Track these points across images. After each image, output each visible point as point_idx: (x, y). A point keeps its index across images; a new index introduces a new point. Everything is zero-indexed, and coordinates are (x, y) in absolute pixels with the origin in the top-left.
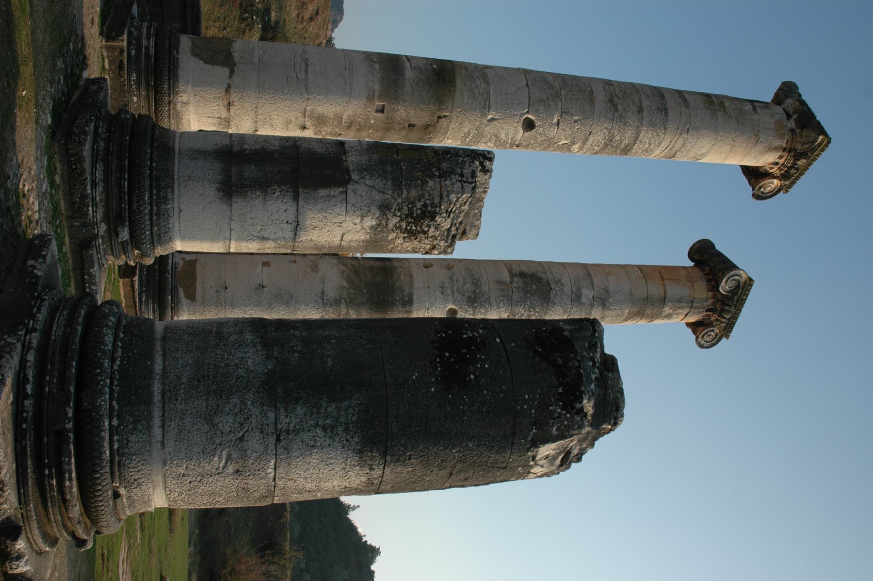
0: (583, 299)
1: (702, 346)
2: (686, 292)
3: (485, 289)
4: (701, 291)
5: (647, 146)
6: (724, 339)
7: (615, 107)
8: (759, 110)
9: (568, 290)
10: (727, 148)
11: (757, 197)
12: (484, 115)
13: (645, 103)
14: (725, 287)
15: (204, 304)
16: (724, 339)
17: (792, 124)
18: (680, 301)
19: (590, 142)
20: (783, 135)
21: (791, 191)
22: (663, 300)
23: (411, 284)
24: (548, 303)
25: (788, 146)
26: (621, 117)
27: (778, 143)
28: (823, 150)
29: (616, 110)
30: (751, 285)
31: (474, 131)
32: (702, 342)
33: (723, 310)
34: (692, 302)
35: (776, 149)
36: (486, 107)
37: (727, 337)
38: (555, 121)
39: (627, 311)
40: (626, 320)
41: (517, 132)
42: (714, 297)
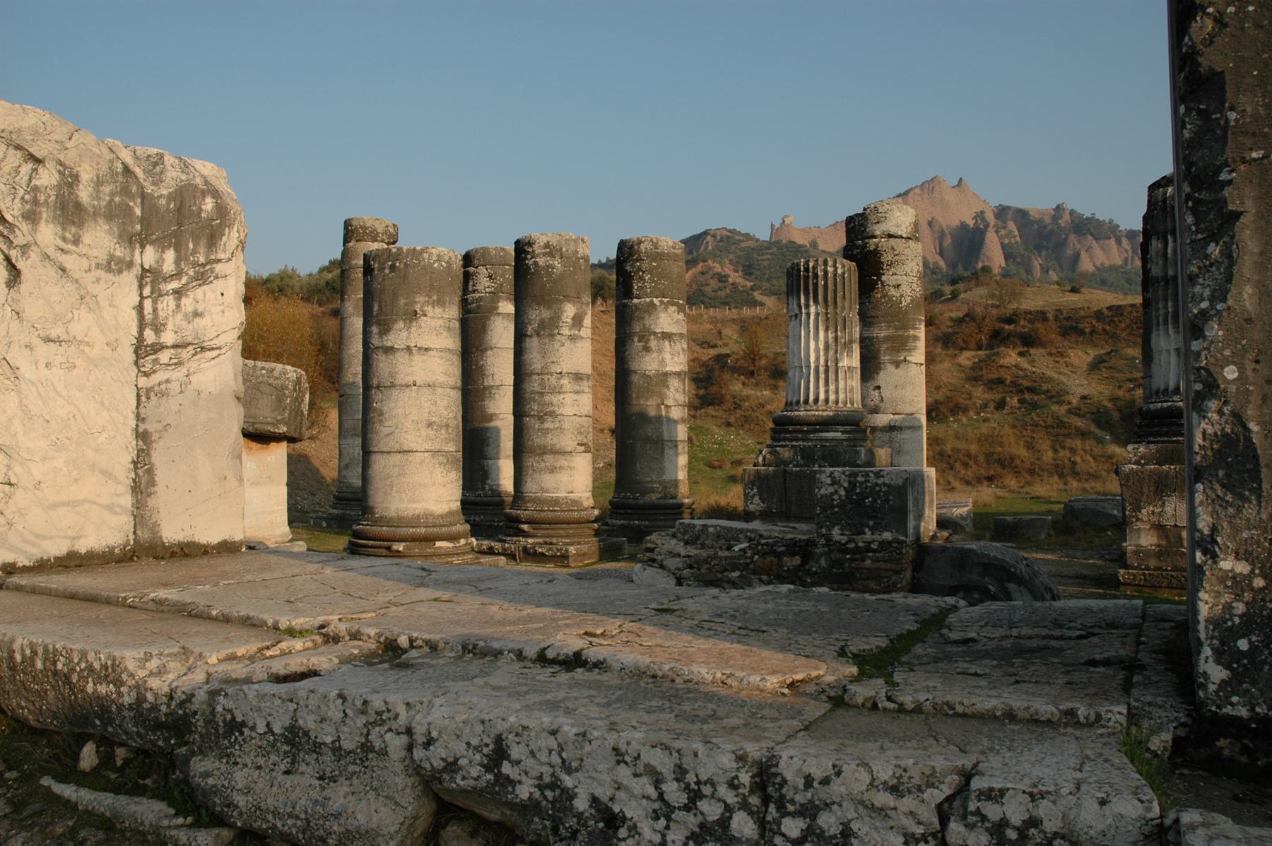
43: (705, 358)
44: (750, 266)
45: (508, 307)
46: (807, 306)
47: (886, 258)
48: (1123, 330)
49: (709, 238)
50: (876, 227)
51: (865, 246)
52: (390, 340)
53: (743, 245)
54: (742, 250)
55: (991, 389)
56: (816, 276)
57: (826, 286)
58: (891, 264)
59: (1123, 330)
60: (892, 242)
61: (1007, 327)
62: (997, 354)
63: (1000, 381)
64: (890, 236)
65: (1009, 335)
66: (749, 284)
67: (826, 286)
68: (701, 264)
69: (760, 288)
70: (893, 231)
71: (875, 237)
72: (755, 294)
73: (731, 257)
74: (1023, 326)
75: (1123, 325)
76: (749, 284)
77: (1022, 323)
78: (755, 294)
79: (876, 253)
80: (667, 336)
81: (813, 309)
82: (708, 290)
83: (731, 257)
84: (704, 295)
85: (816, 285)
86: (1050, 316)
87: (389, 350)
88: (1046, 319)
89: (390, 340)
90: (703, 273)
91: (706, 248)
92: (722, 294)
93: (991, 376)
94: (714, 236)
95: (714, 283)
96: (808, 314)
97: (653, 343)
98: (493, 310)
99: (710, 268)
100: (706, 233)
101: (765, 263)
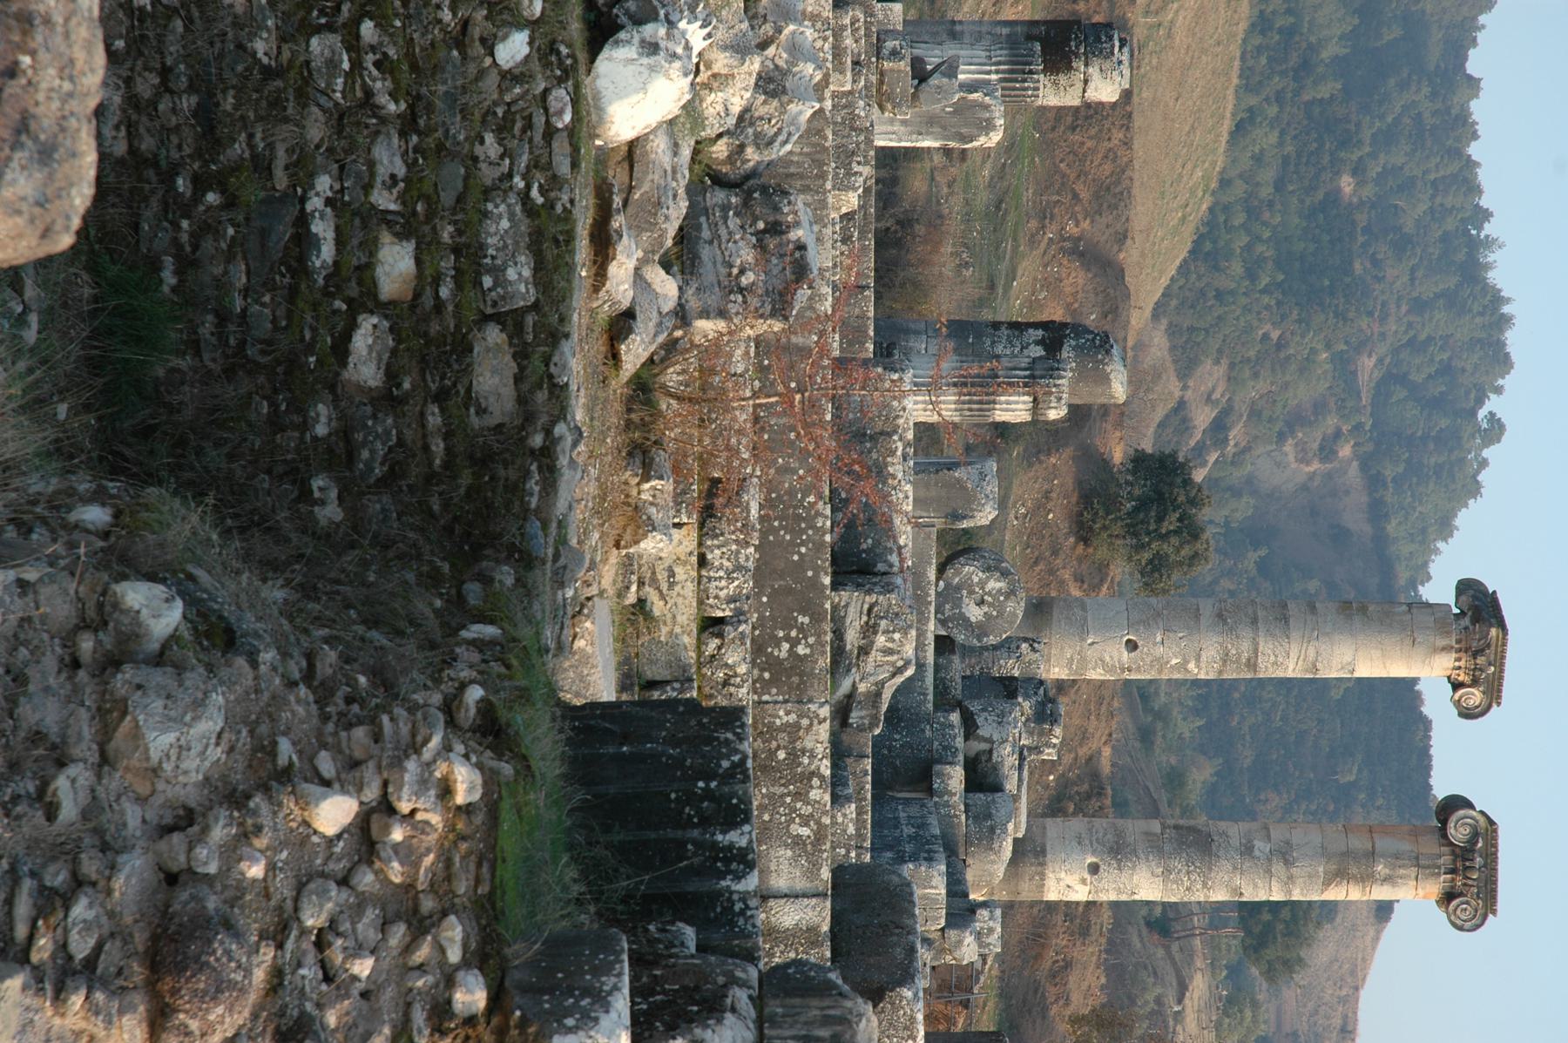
0: (1257, 853)
1: (1461, 928)
2: (1406, 846)
3: (1131, 839)
4: (1430, 846)
5: (1272, 658)
6: (1491, 916)
7: (1225, 622)
8: (1414, 611)
9: (1235, 842)
10: (1376, 653)
11: (1467, 714)
12: (1084, 640)
13: (1260, 613)
14: (1458, 832)
16: (1491, 916)
17: (1466, 621)
18: (1397, 856)
19: (1204, 658)
20: (1448, 633)
21: (1504, 700)
22: (1372, 855)
23: (1044, 834)
24: (1210, 855)
25: (1463, 645)
26: (1231, 629)
27: (1441, 642)
28: (1504, 644)
29: (1225, 622)
30: (1495, 831)
31: (1077, 657)
32: (1459, 922)
33: (1466, 868)
34: (1417, 858)
36: (1083, 630)
37: (1494, 912)
38: (1159, 639)
39: (1321, 869)
41: (1121, 654)
42: (1453, 853)
46: (997, 72)
47: (1062, 79)
50: (1097, 68)
51: (1077, 55)
56: (1024, 81)
57: (1015, 89)
58: (1055, 83)
60: (1080, 85)
64: (1086, 82)
67: (1015, 89)
70: (1092, 85)
71: (1086, 65)
79: (1069, 68)
81: (994, 77)
85: (1016, 81)
96: (989, 73)
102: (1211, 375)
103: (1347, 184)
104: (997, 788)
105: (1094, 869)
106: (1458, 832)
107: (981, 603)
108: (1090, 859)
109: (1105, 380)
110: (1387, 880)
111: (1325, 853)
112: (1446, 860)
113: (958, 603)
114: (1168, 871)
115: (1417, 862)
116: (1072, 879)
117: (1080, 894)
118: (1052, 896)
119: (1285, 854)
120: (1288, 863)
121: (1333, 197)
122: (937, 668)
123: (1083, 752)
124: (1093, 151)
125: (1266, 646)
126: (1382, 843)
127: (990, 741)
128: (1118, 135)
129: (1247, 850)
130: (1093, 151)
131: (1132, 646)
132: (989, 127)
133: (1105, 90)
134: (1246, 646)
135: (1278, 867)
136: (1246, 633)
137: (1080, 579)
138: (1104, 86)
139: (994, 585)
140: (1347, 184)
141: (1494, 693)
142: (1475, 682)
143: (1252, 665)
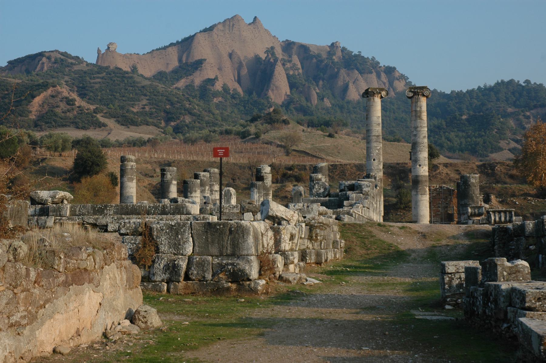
4: (414, 99)
10: (375, 112)
15: (417, 219)
18: (416, 106)
22: (416, 111)
27: (372, 100)
35: (373, 99)
40: (422, 119)
43: (154, 184)
44: (84, 88)
45: (175, 182)
47: (265, 177)
48: (337, 175)
49: (44, 59)
52: (192, 195)
53: (76, 68)
54: (75, 72)
55: (283, 200)
59: (337, 175)
61: (289, 172)
62: (285, 186)
63: (286, 197)
65: (290, 176)
66: (92, 107)
68: (51, 89)
69: (102, 111)
72: (98, 116)
73: (67, 78)
74: (296, 172)
75: (337, 173)
76: (92, 107)
77: (296, 170)
78: (98, 116)
79: (263, 176)
80: (216, 191)
82: (58, 111)
83: (67, 78)
84: (55, 115)
86: (307, 168)
87: (192, 197)
88: (305, 169)
89: (192, 195)
90: (53, 96)
91: (42, 68)
92: (70, 115)
93: (282, 195)
94: (49, 58)
95: (63, 106)
97: (214, 192)
98: (171, 183)
99: (59, 93)
100: (41, 55)
101: (97, 86)
102: (502, 144)
103: (464, 117)
104: (353, 185)
105: (420, 165)
106: (411, 94)
107: (320, 189)
108: (418, 166)
109: (322, 167)
110: (421, 108)
111: (415, 120)
112: (416, 97)
113: (320, 193)
114: (420, 151)
115: (417, 102)
116: (422, 170)
117: (426, 168)
118: (427, 174)
119: (416, 128)
120: (417, 127)
121: (467, 120)
122: (333, 197)
123: (475, 168)
124: (350, 171)
125: (374, 134)
126: (414, 109)
127: (345, 187)
128: (348, 166)
129: (415, 135)
130: (350, 171)
131: (374, 160)
132: (229, 190)
133: (267, 169)
134: (374, 138)
135: (419, 129)
136: (371, 138)
137: (435, 171)
138: (267, 169)
139: (316, 187)
140: (464, 117)
141: (382, 90)
142: (380, 93)
143: (378, 136)
